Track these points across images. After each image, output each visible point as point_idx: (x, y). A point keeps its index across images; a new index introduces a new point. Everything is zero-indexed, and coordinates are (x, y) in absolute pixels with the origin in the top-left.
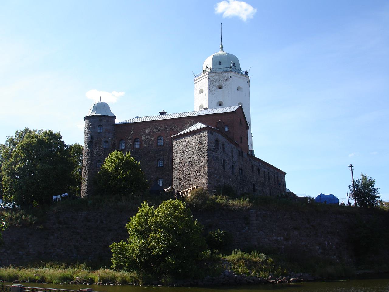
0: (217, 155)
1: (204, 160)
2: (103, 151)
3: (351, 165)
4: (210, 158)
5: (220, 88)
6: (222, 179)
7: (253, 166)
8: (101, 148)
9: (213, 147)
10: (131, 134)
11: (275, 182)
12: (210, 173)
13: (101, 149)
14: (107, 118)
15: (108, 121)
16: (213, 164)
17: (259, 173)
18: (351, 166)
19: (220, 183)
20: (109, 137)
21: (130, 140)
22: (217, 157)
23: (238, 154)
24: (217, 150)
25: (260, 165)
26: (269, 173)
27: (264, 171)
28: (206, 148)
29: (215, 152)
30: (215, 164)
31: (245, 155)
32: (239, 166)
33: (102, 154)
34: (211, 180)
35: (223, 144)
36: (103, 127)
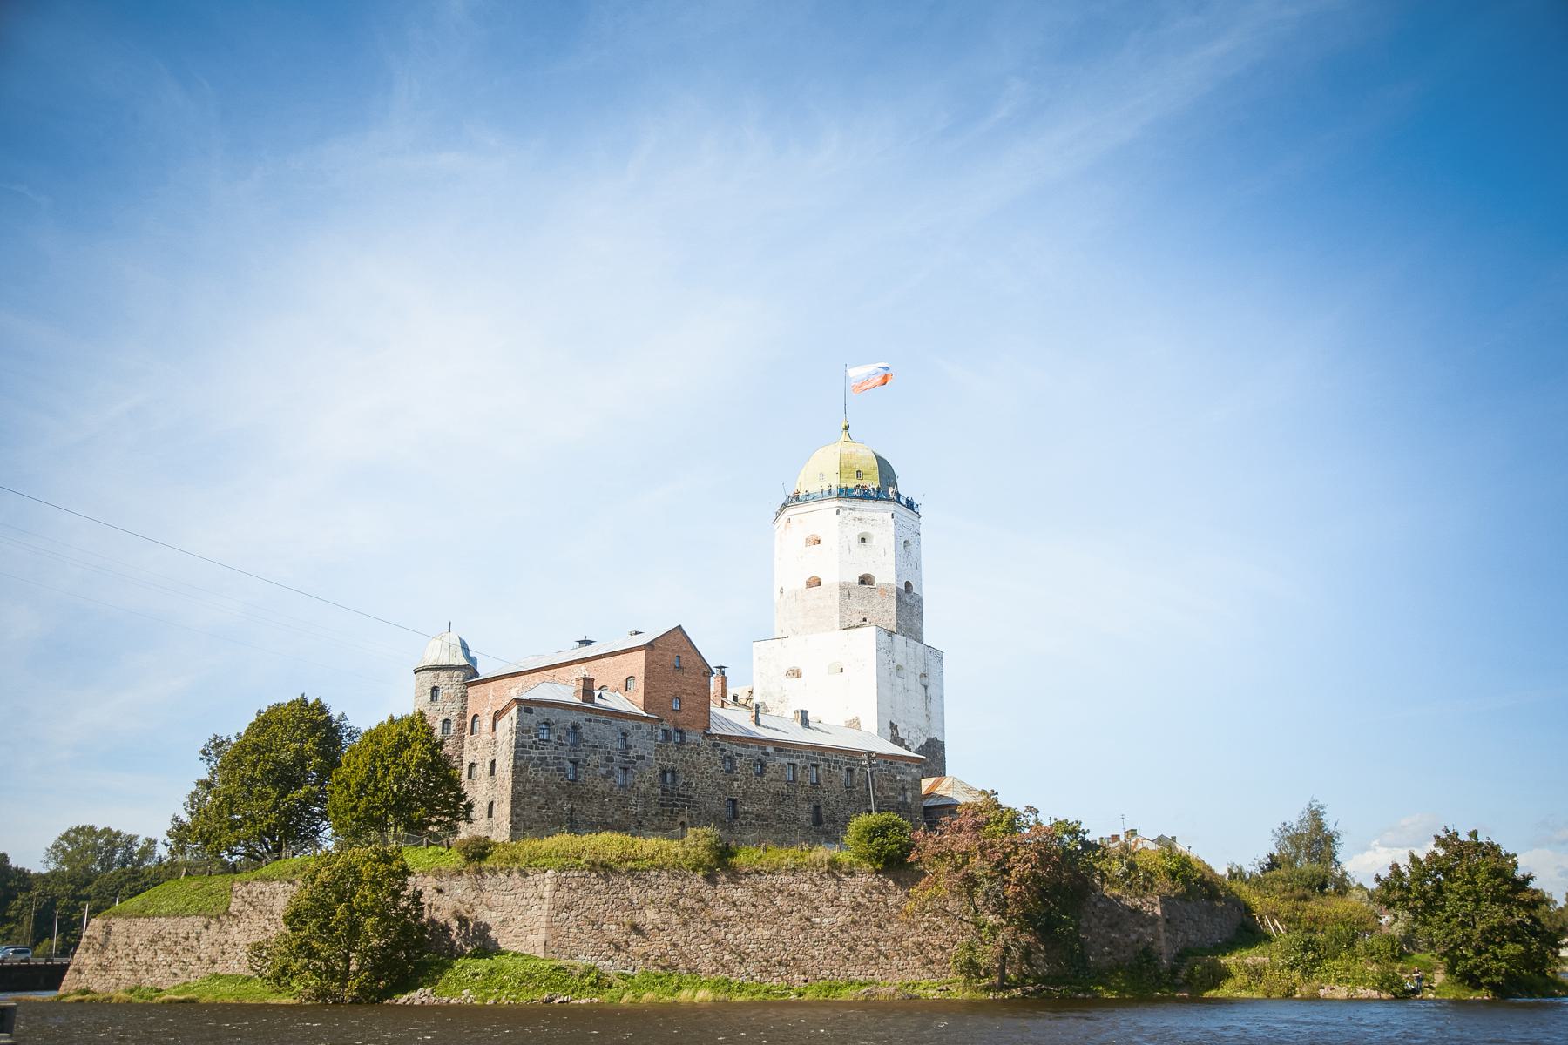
0: (540, 753)
1: (511, 765)
6: (558, 803)
9: (531, 738)
15: (451, 677)
16: (531, 773)
17: (761, 774)
25: (767, 754)
29: (537, 748)
30: (536, 775)
32: (660, 764)
35: (575, 727)
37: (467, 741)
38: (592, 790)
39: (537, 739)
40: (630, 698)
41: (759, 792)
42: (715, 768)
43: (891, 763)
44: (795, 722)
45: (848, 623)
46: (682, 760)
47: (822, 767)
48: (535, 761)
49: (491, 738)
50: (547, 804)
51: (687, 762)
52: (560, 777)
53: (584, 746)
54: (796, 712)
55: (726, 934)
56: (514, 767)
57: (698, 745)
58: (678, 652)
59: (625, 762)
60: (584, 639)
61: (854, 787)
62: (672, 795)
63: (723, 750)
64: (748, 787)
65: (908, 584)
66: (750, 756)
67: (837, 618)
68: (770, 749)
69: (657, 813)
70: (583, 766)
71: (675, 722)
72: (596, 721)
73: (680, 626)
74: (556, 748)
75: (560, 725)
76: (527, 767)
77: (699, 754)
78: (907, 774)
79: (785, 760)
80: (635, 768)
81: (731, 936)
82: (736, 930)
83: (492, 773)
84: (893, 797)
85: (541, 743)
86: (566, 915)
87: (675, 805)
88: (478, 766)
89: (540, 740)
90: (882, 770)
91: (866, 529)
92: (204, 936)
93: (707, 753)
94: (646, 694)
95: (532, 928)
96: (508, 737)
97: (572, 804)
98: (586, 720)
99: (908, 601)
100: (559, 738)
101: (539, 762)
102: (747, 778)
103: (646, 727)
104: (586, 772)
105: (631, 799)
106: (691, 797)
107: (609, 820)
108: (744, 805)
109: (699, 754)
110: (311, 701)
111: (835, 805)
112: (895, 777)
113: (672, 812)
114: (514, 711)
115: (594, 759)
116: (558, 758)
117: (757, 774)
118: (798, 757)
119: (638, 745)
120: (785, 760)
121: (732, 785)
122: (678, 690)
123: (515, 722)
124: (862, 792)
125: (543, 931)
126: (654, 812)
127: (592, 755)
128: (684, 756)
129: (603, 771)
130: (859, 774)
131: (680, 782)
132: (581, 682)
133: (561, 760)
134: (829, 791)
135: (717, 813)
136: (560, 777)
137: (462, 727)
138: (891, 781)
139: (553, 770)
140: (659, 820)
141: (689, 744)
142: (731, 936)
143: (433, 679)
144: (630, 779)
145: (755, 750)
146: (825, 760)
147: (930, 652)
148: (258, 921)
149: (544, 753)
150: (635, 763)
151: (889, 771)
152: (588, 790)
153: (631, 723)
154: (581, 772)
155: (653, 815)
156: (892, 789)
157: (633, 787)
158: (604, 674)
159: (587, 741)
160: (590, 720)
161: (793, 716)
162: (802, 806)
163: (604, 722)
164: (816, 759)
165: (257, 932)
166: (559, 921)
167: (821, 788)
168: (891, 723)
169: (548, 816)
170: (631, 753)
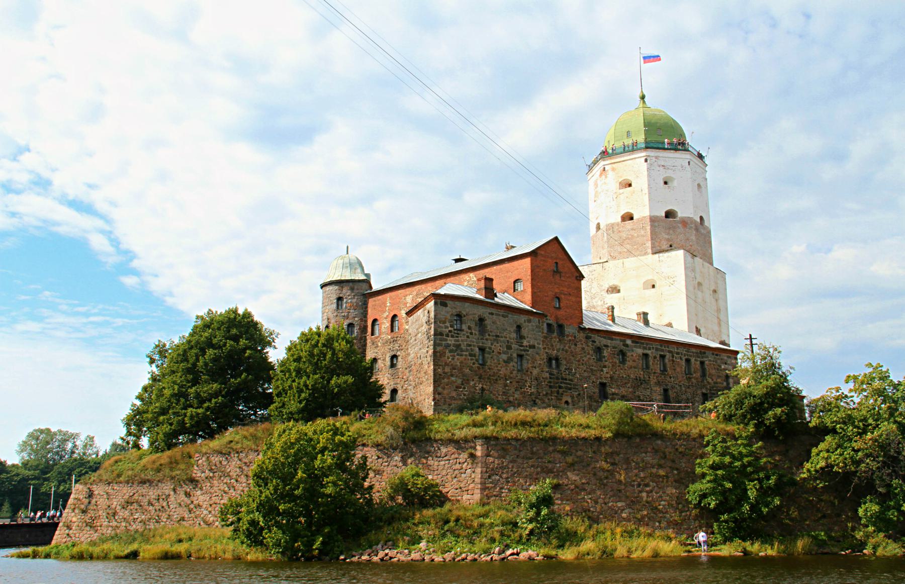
1: (431, 352)
3: (750, 335)
4: (438, 349)
5: (630, 185)
6: (472, 383)
7: (599, 350)
10: (387, 308)
11: (688, 373)
12: (440, 375)
14: (351, 284)
16: (448, 358)
17: (623, 361)
18: (751, 338)
19: (467, 391)
21: (386, 318)
22: (458, 346)
23: (545, 331)
24: (459, 332)
25: (627, 346)
26: (663, 357)
27: (646, 356)
28: (432, 332)
29: (452, 336)
30: (453, 359)
31: (569, 330)
32: (547, 353)
34: (444, 388)
35: (481, 320)
37: (369, 341)
38: (497, 373)
39: (452, 329)
40: (519, 297)
41: (623, 377)
42: (588, 356)
43: (717, 355)
44: (638, 323)
45: (658, 248)
46: (563, 350)
47: (667, 357)
48: (452, 347)
49: (390, 337)
50: (462, 384)
51: (566, 351)
52: (472, 361)
53: (489, 335)
54: (639, 314)
55: (641, 492)
56: (435, 352)
57: (575, 337)
58: (556, 259)
59: (521, 350)
60: (458, 257)
61: (692, 374)
62: (558, 378)
63: (594, 342)
64: (614, 373)
65: (701, 218)
66: (614, 347)
67: (649, 244)
68: (629, 342)
69: (547, 394)
70: (489, 353)
71: (557, 319)
72: (497, 315)
73: (556, 239)
74: (468, 337)
75: (471, 317)
76: (445, 352)
77: (576, 345)
78: (729, 365)
79: (640, 351)
80: (527, 355)
81: (644, 494)
82: (648, 489)
83: (393, 365)
84: (720, 383)
85: (456, 332)
86: (497, 477)
87: (560, 387)
88: (379, 361)
89: (455, 330)
90: (710, 361)
91: (669, 173)
92: (172, 498)
93: (582, 344)
94: (533, 293)
95: (466, 488)
96: (425, 328)
97: (483, 384)
98: (490, 314)
99: (703, 231)
100: (470, 328)
101: (454, 348)
102: (613, 366)
103: (535, 320)
104: (492, 358)
105: (526, 381)
106: (571, 380)
107: (511, 399)
108: (612, 388)
109: (576, 345)
110: (241, 312)
111: (679, 388)
112: (720, 366)
113: (558, 392)
114: (431, 305)
115: (497, 347)
116: (470, 345)
117: (620, 362)
118: (650, 349)
119: (529, 336)
120: (640, 351)
121: (602, 371)
122: (557, 290)
123: (432, 315)
124: (697, 379)
125: (479, 491)
126: (545, 393)
127: (495, 344)
128: (565, 347)
129: (505, 357)
130: (695, 364)
131: (563, 368)
132: (483, 281)
133: (472, 347)
134: (673, 377)
135: (592, 393)
136: (472, 361)
137: (364, 329)
138: (718, 369)
139: (466, 355)
140: (548, 399)
141: (568, 336)
142: (644, 494)
143: (337, 291)
144: (525, 365)
145: (617, 342)
146: (670, 352)
147: (718, 273)
148: (217, 485)
149: (458, 341)
150: (528, 351)
151: (716, 362)
152: (494, 372)
153: (522, 319)
154: (488, 357)
155: (544, 395)
156: (719, 377)
157: (527, 371)
158: (501, 278)
159: (491, 332)
160: (492, 314)
161: (636, 317)
162: (655, 389)
163: (503, 316)
164: (663, 351)
165: (217, 494)
166: (491, 483)
167: (668, 374)
168: (697, 328)
169: (465, 395)
170: (525, 343)
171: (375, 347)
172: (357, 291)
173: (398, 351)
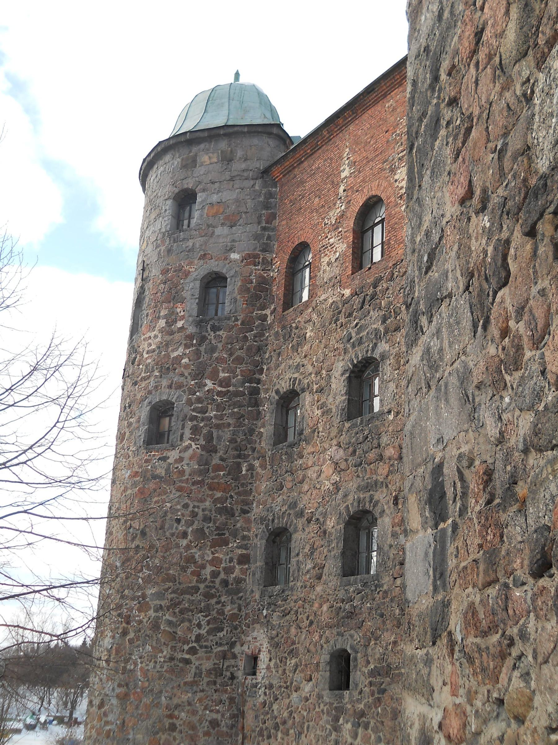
2: (190, 337)
8: (180, 324)
13: (182, 328)
14: (223, 145)
20: (231, 249)
33: (185, 361)
36: (200, 197)
171: (295, 349)
172: (243, 166)
173: (378, 336)
